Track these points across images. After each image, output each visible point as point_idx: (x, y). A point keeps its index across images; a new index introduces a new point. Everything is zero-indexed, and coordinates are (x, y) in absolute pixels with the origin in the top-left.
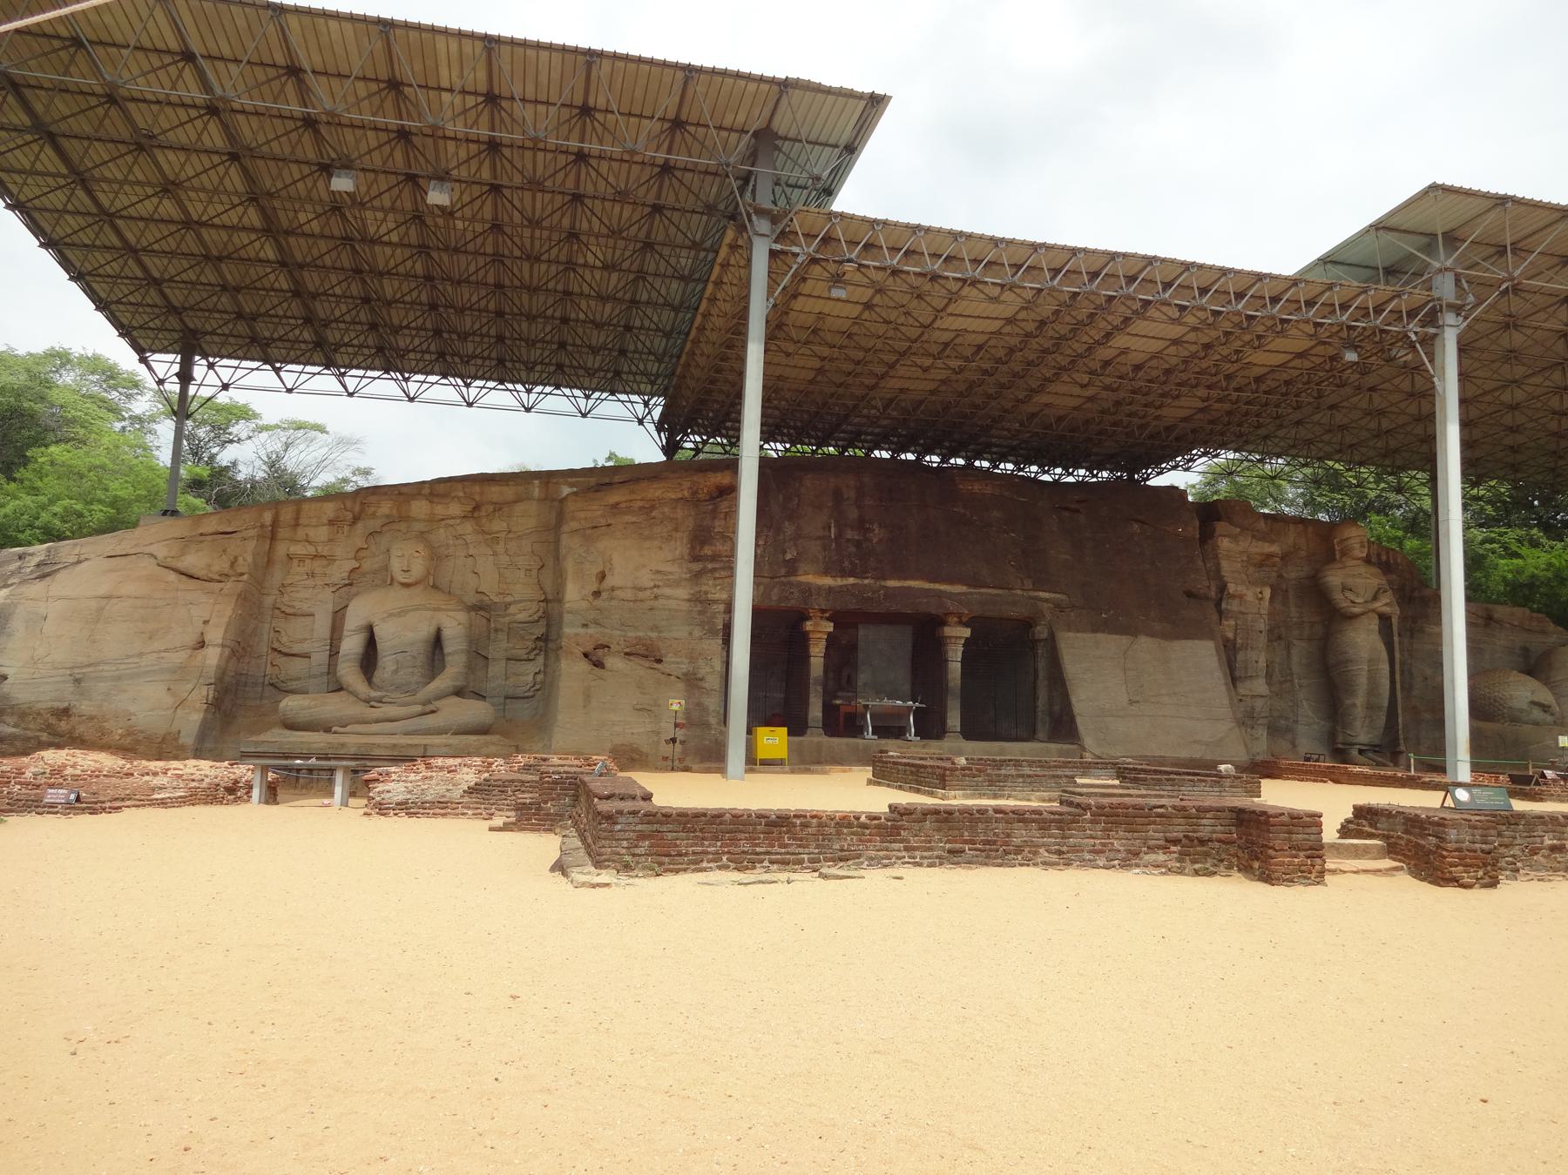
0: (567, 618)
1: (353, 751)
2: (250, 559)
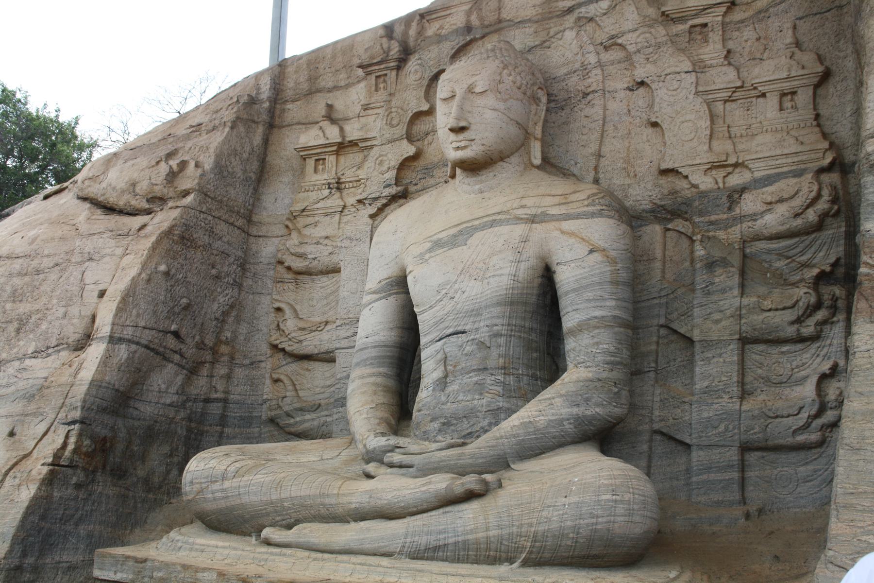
2: (208, 163)
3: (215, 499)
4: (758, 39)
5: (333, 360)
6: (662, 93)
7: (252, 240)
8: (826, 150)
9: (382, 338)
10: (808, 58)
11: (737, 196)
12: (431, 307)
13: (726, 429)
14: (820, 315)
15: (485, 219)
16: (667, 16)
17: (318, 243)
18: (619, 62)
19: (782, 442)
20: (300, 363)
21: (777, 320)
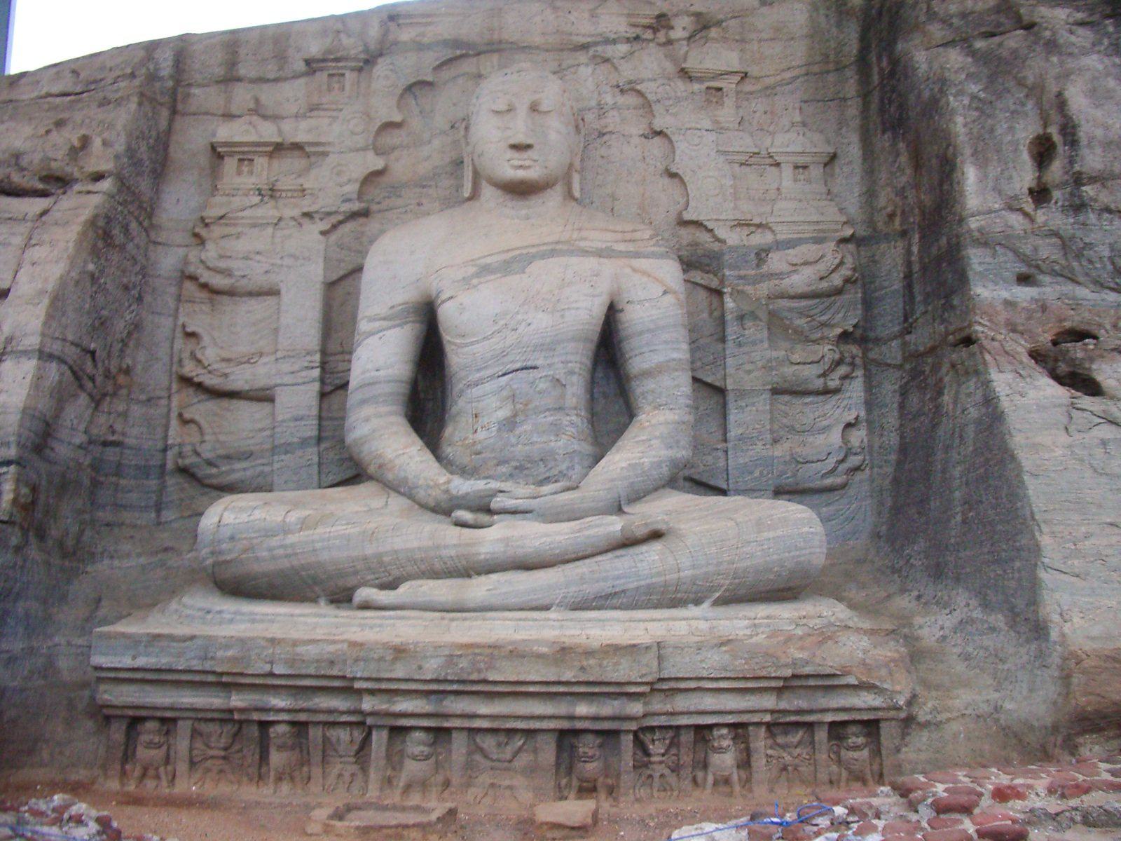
0: (976, 258)
1: (432, 667)
3: (274, 558)
4: (765, 113)
5: (271, 400)
6: (681, 146)
7: (151, 247)
8: (845, 223)
9: (396, 372)
10: (817, 137)
11: (764, 255)
12: (485, 339)
13: (761, 473)
14: (843, 370)
15: (545, 248)
16: (686, 73)
17: (247, 258)
18: (634, 108)
19: (811, 485)
20: (218, 401)
21: (806, 373)
